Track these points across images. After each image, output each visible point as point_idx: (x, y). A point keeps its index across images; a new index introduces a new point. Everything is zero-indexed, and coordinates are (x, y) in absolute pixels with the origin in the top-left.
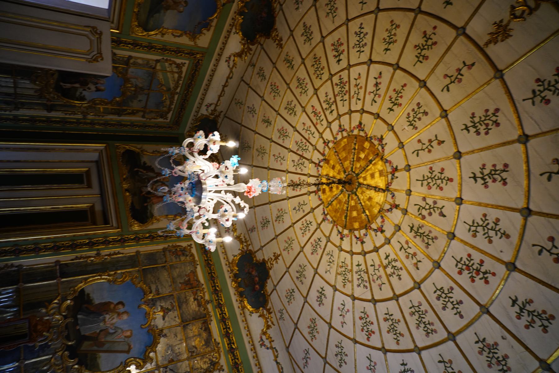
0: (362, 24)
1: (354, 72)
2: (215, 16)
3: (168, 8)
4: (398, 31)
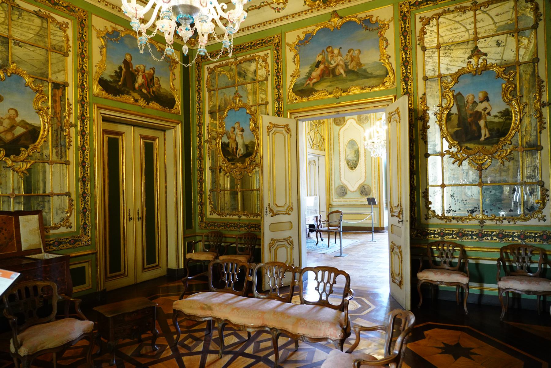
3: (359, 64)
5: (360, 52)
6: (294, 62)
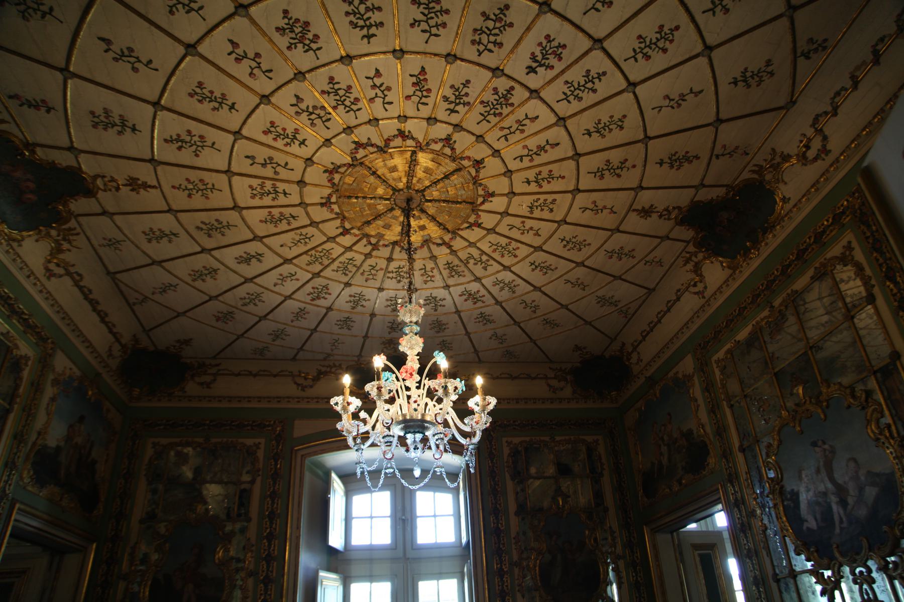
0: (604, 74)
1: (534, 107)
4: (616, 131)
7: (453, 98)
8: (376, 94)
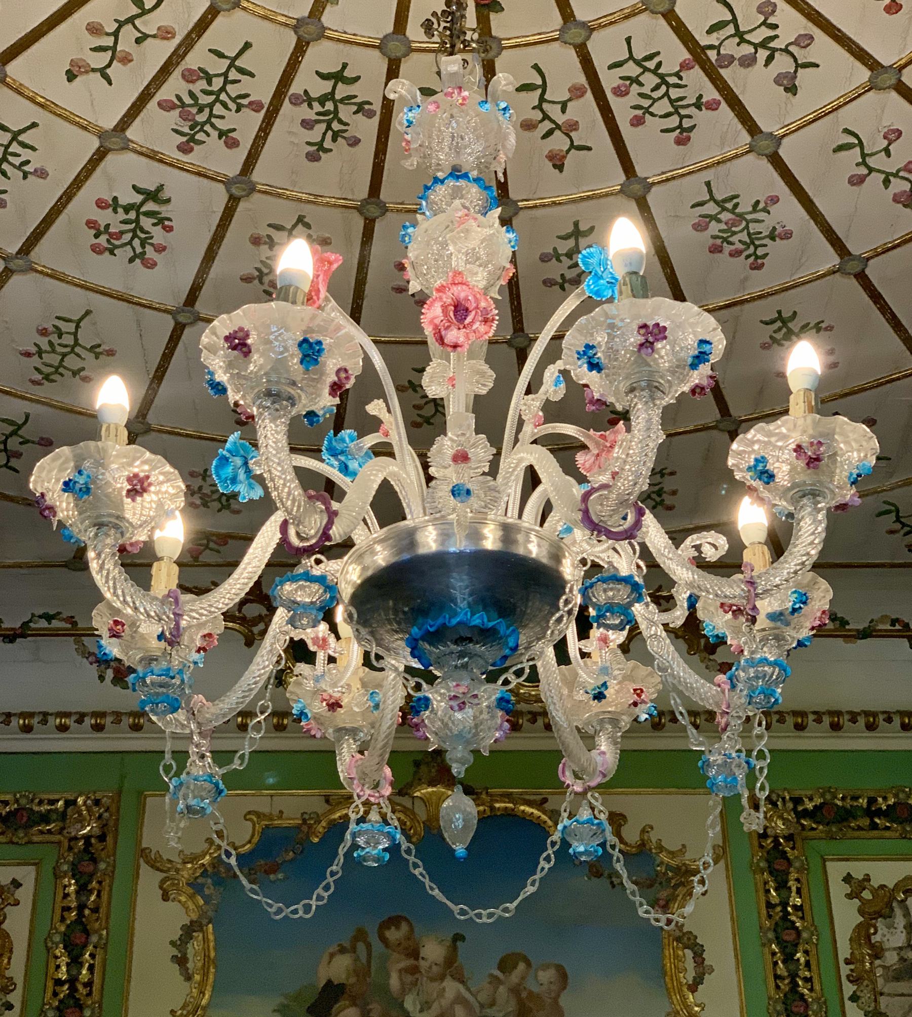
2: (536, 812)
5: (563, 976)
6: (181, 961)
7: (345, 112)
8: (564, 110)
